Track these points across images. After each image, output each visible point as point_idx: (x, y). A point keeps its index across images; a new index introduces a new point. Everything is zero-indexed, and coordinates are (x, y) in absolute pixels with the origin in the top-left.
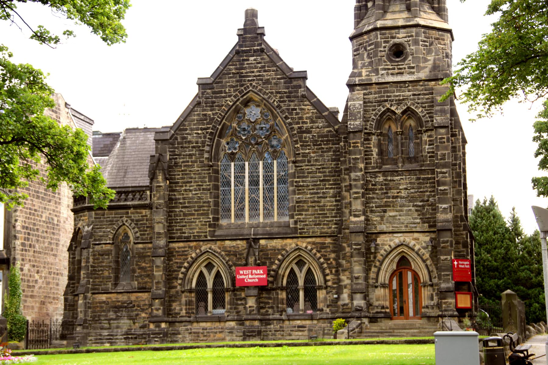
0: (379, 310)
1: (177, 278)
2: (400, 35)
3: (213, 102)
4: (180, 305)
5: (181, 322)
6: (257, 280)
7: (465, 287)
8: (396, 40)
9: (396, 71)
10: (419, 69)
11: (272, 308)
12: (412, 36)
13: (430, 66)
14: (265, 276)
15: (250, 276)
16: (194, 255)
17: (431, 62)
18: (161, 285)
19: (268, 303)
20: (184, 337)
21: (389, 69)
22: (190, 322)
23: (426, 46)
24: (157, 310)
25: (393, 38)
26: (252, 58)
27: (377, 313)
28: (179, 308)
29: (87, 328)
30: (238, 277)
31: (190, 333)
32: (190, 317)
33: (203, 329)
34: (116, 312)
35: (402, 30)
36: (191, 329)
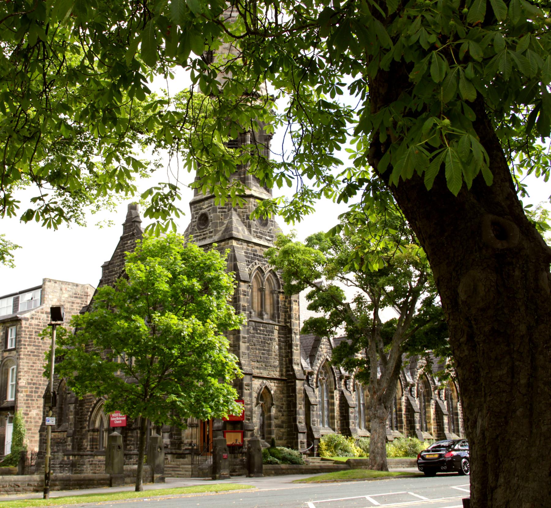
0: (187, 447)
1: (86, 421)
2: (204, 207)
3: (109, 280)
4: (87, 441)
5: (87, 455)
6: (120, 422)
7: (239, 426)
8: (203, 211)
9: (202, 237)
10: (216, 232)
11: (133, 444)
12: (211, 206)
13: (223, 229)
14: (124, 418)
15: (118, 419)
16: (95, 402)
17: (225, 226)
18: (73, 426)
19: (131, 441)
20: (87, 468)
21: (198, 236)
22: (91, 455)
23: (224, 212)
24: (69, 445)
25: (201, 209)
26: (129, 242)
27: (186, 449)
28: (86, 444)
29: (42, 458)
30: (112, 419)
31: (91, 464)
32: (92, 451)
33: (99, 461)
34: (57, 446)
35: (206, 202)
36: (92, 461)
